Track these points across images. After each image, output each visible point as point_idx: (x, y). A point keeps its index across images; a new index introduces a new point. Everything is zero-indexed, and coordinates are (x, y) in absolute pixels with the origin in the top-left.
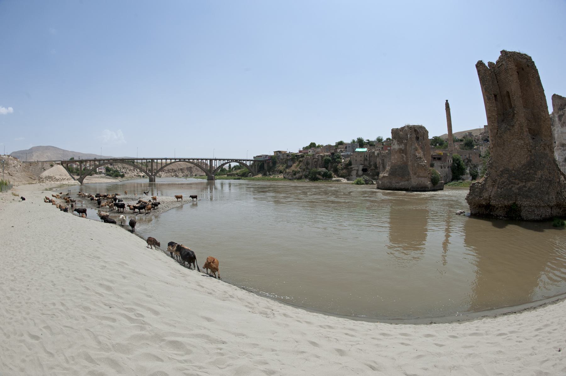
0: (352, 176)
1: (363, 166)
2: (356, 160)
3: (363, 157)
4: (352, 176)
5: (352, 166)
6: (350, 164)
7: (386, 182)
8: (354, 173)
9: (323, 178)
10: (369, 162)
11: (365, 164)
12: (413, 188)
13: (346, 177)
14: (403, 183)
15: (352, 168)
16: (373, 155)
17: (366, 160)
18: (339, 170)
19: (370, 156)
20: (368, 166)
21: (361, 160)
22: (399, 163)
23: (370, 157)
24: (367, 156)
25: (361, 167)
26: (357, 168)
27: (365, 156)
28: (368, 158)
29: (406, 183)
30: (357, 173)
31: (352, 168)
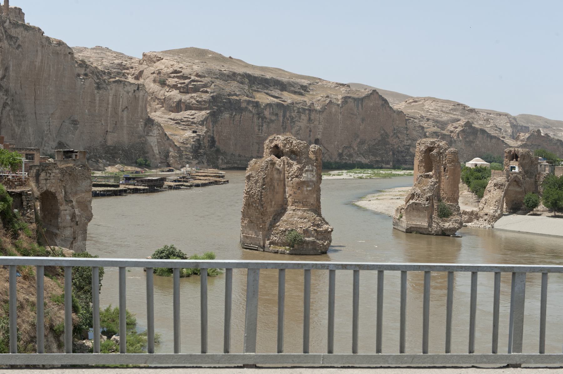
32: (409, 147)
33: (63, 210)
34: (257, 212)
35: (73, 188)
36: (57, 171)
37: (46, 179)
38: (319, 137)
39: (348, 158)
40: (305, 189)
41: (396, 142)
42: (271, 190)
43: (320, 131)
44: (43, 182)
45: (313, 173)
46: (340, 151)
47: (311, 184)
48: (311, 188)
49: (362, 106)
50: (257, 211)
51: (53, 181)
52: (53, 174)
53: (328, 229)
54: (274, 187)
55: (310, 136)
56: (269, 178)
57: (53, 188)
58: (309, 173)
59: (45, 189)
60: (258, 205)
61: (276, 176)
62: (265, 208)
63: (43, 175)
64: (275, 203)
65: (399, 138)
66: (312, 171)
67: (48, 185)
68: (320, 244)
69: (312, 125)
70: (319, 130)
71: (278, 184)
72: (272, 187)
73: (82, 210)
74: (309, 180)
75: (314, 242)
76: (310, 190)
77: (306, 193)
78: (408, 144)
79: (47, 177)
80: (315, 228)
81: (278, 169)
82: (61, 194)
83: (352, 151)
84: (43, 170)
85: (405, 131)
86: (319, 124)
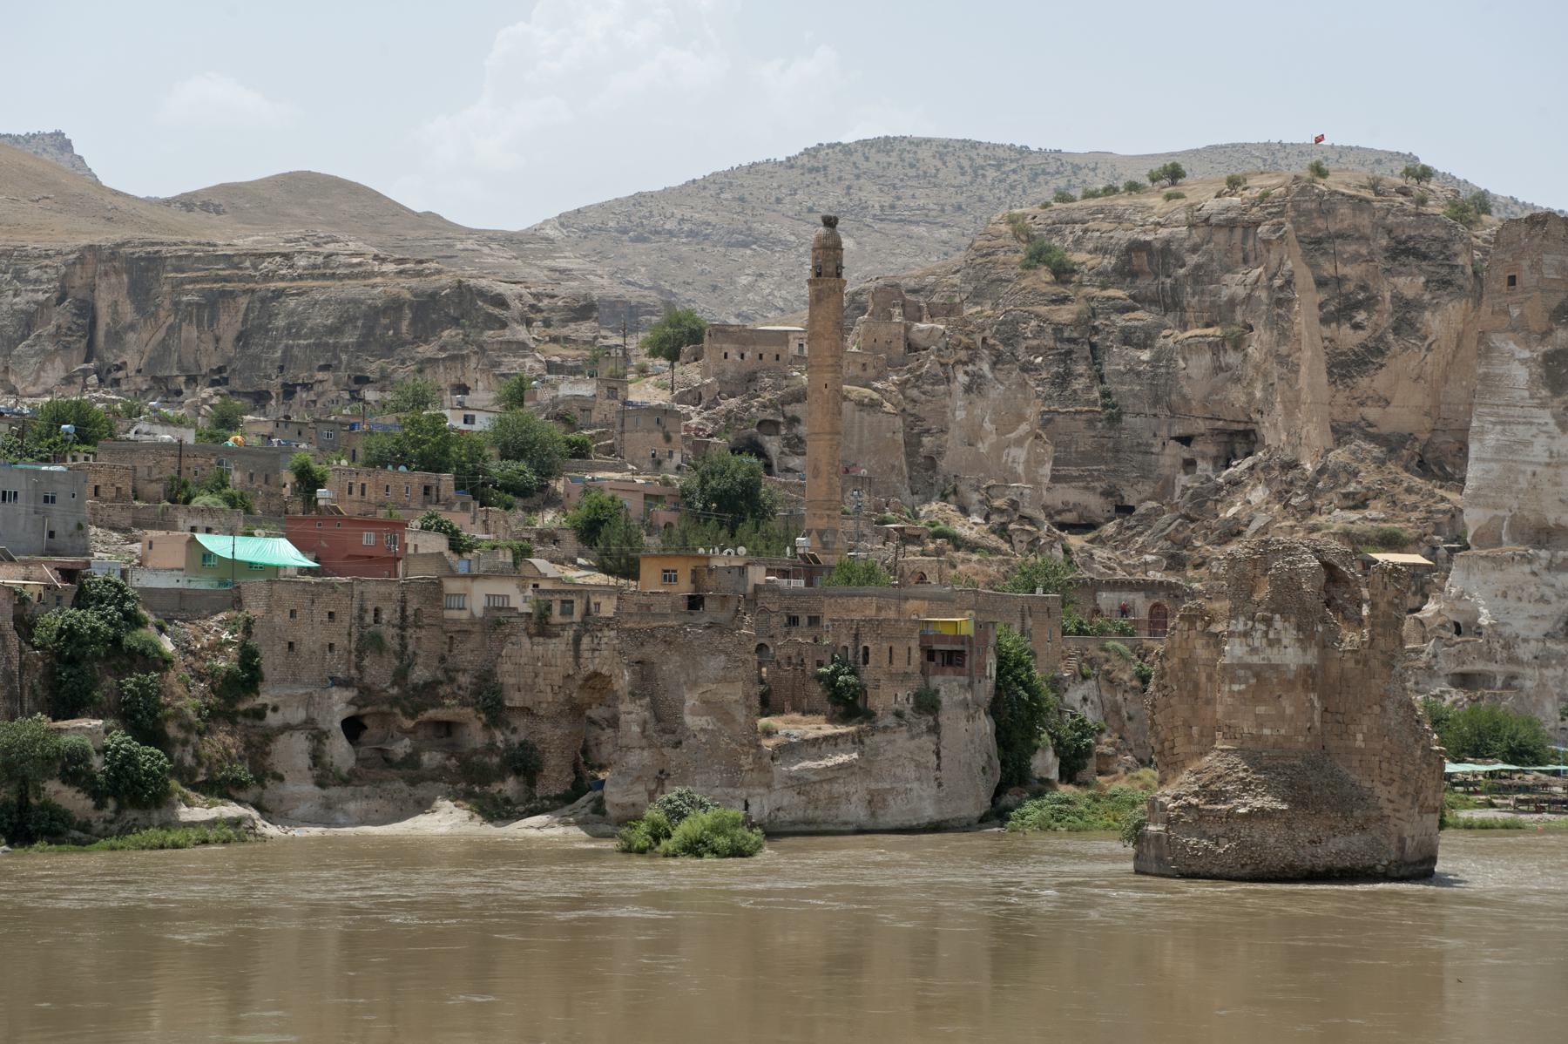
0: (281, 778)
1: (350, 694)
2: (291, 645)
3: (345, 620)
4: (281, 778)
5: (265, 697)
6: (248, 676)
7: (1272, 840)
8: (292, 753)
9: (100, 806)
10: (397, 663)
11: (367, 680)
12: (1407, 864)
13: (242, 795)
14: (1340, 843)
15: (259, 714)
16: (427, 610)
17: (370, 643)
18: (187, 727)
19: (404, 617)
20: (394, 701)
21: (331, 646)
22: (1301, 739)
23: (403, 628)
24: (385, 617)
25: (339, 705)
26: (300, 715)
27: (369, 618)
28: (389, 634)
29: (1358, 841)
30: (316, 758)
31: (259, 714)
35: (691, 671)
36: (613, 633)
37: (594, 650)
40: (1227, 689)
42: (1185, 694)
44: (587, 654)
45: (1250, 641)
47: (1241, 673)
48: (1243, 687)
51: (606, 653)
52: (605, 640)
53: (1236, 808)
54: (1197, 686)
56: (1175, 660)
57: (605, 668)
58: (1237, 641)
59: (591, 668)
61: (1202, 652)
62: (1166, 744)
63: (586, 640)
64: (1202, 731)
66: (1246, 634)
67: (597, 661)
68: (1192, 849)
71: (1210, 678)
72: (1190, 686)
73: (718, 720)
74: (1235, 661)
75: (1158, 837)
76: (1240, 692)
77: (1230, 701)
79: (594, 646)
80: (1194, 801)
81: (1216, 635)
82: (621, 681)
84: (587, 631)
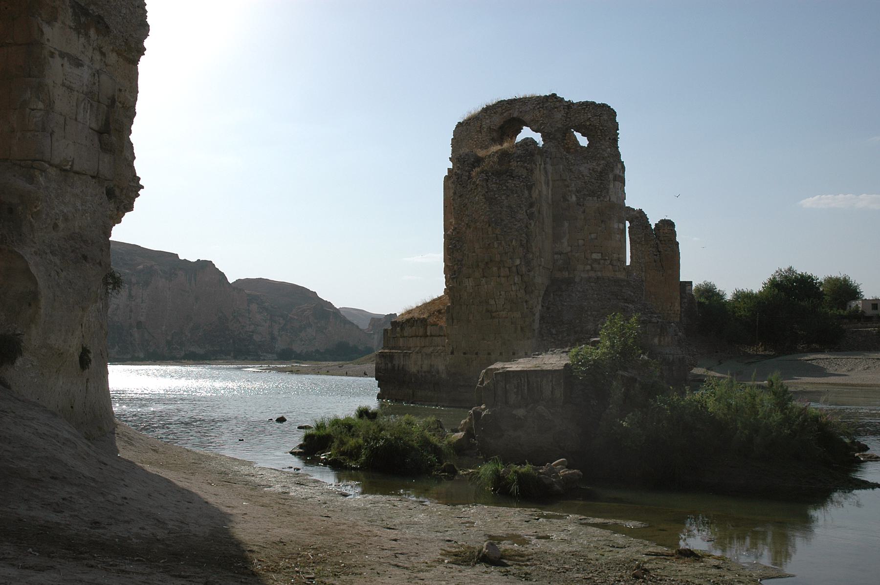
32: (251, 334)
33: (62, 55)
34: (515, 284)
38: (142, 319)
39: (179, 347)
41: (236, 328)
43: (143, 312)
46: (169, 338)
49: (195, 281)
50: (516, 279)
55: (130, 318)
60: (518, 262)
65: (240, 323)
69: (133, 303)
70: (143, 310)
78: (251, 330)
83: (184, 339)
85: (247, 314)
86: (142, 302)
